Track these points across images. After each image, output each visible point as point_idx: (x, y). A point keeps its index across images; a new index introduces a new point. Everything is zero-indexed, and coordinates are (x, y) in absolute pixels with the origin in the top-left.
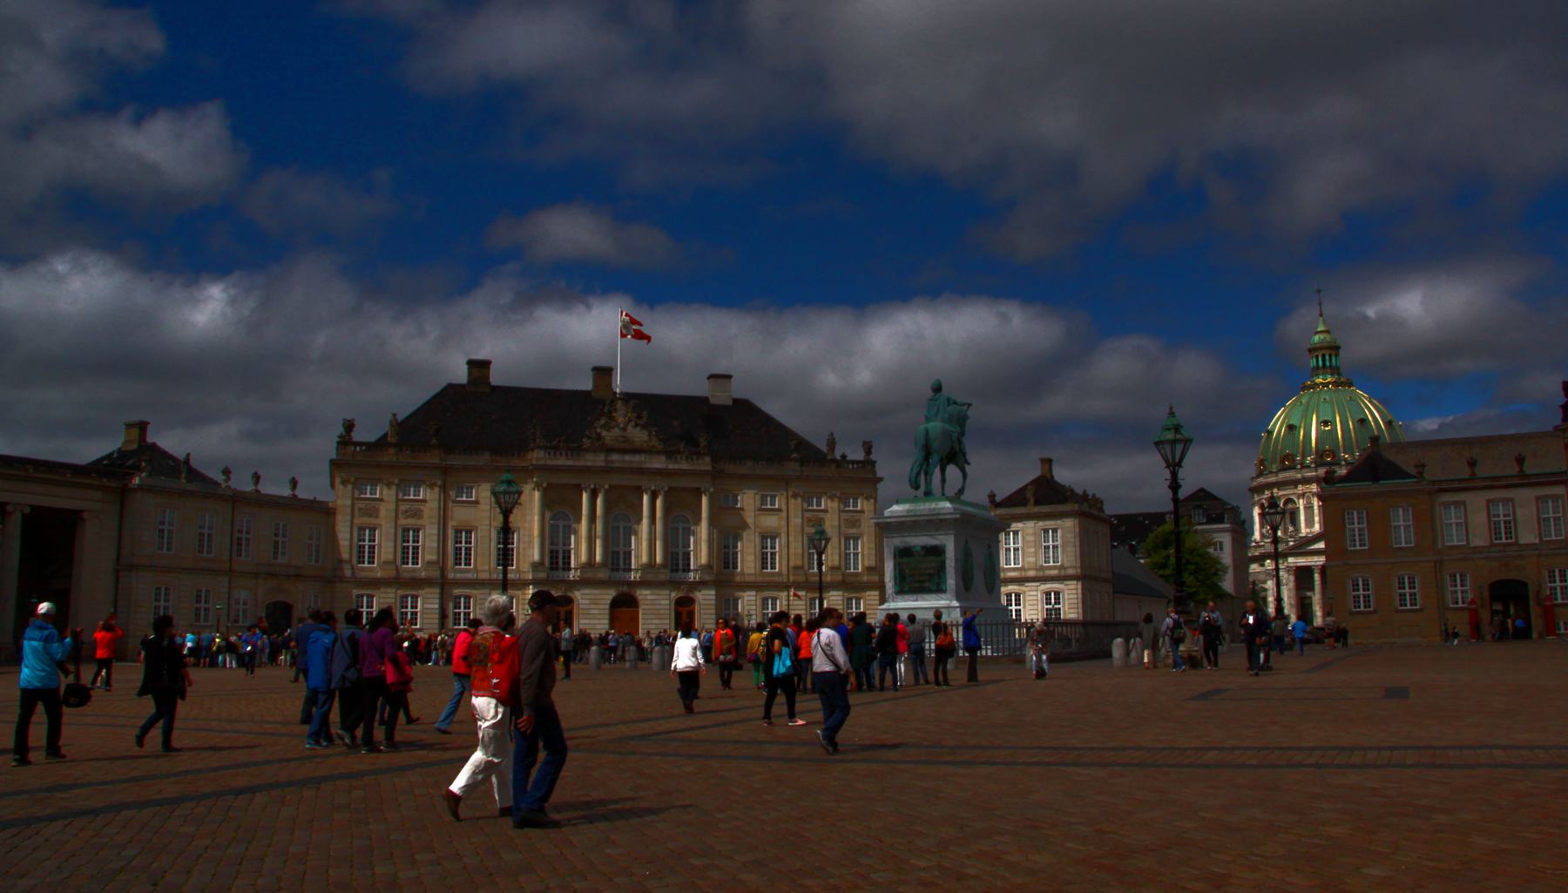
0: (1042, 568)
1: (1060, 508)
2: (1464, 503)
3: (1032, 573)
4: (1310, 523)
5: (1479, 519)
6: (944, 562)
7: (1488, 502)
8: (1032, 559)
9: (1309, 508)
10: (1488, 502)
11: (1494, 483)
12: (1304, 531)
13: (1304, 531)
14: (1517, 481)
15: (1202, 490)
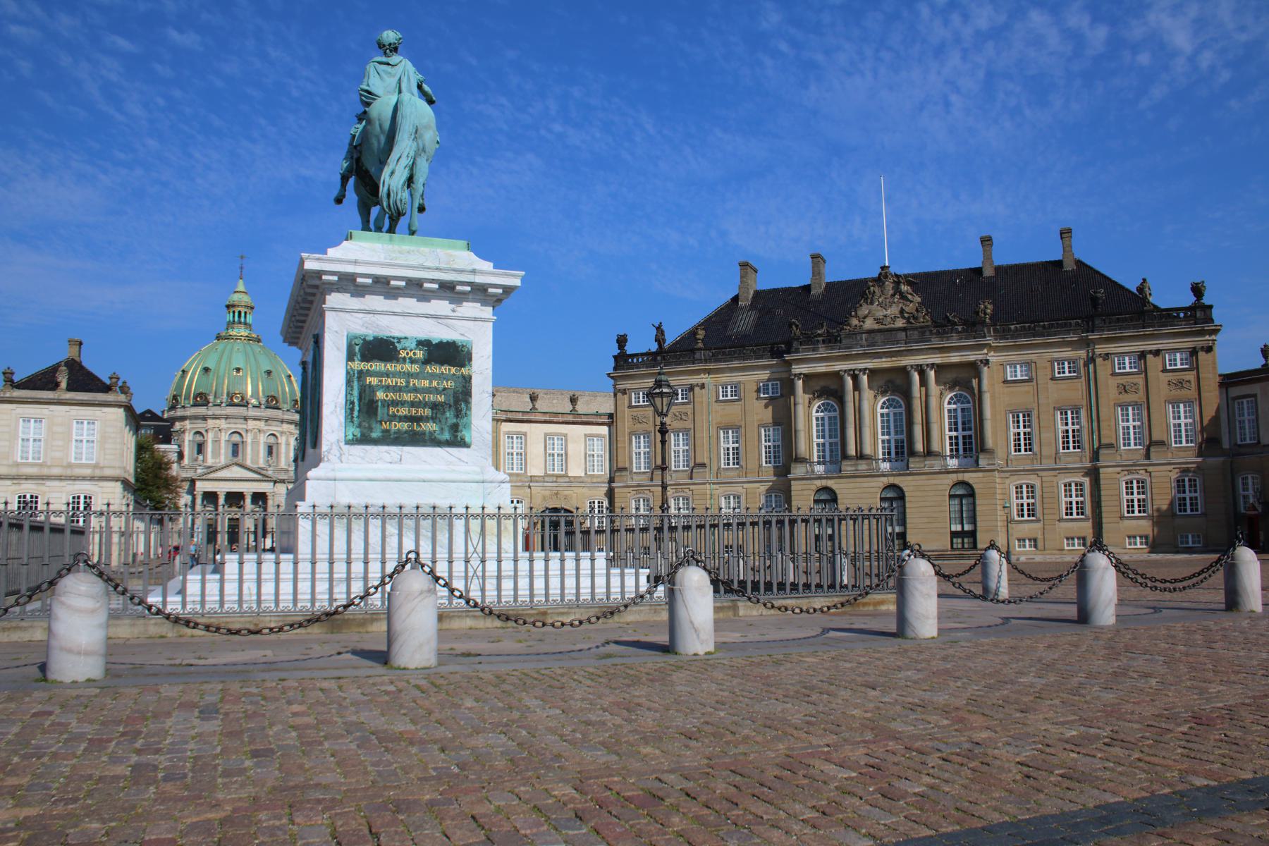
0: (70, 466)
1: (101, 397)
2: (525, 434)
3: (56, 471)
4: (216, 454)
5: (536, 450)
6: (467, 380)
7: (546, 435)
8: (58, 454)
9: (217, 441)
10: (546, 435)
11: (552, 418)
12: (210, 461)
13: (210, 461)
14: (570, 418)
15: (149, 411)
